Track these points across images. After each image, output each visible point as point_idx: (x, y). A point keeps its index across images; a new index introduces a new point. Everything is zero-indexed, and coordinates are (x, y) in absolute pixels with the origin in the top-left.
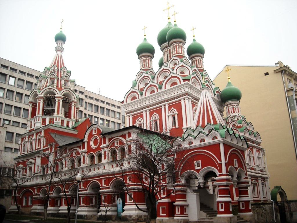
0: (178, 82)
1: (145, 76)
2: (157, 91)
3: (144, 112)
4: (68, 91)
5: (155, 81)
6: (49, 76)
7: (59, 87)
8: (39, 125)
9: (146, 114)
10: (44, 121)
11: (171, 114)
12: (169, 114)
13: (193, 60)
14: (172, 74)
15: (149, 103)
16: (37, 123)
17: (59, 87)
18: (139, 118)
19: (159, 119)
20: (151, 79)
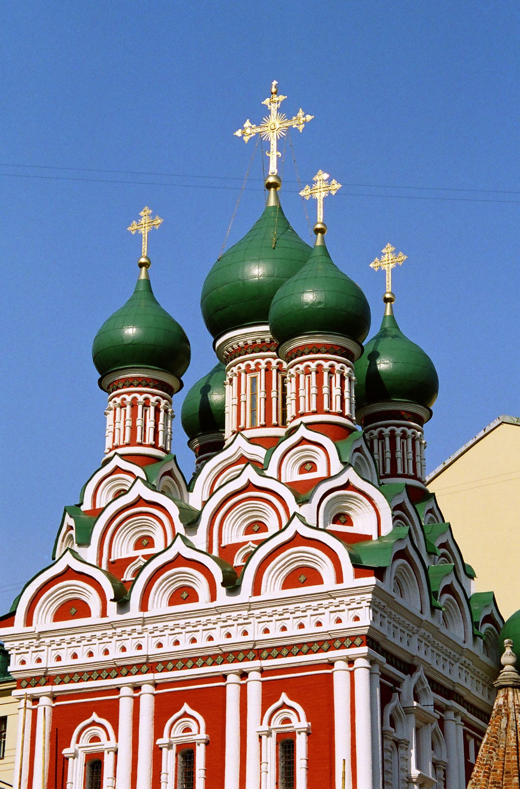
0: (327, 570)
1: (139, 501)
3: (126, 691)
5: (199, 539)
9: (137, 701)
11: (272, 726)
12: (265, 727)
13: (376, 433)
14: (296, 526)
15: (160, 650)
18: (95, 717)
19: (207, 744)
20: (180, 528)
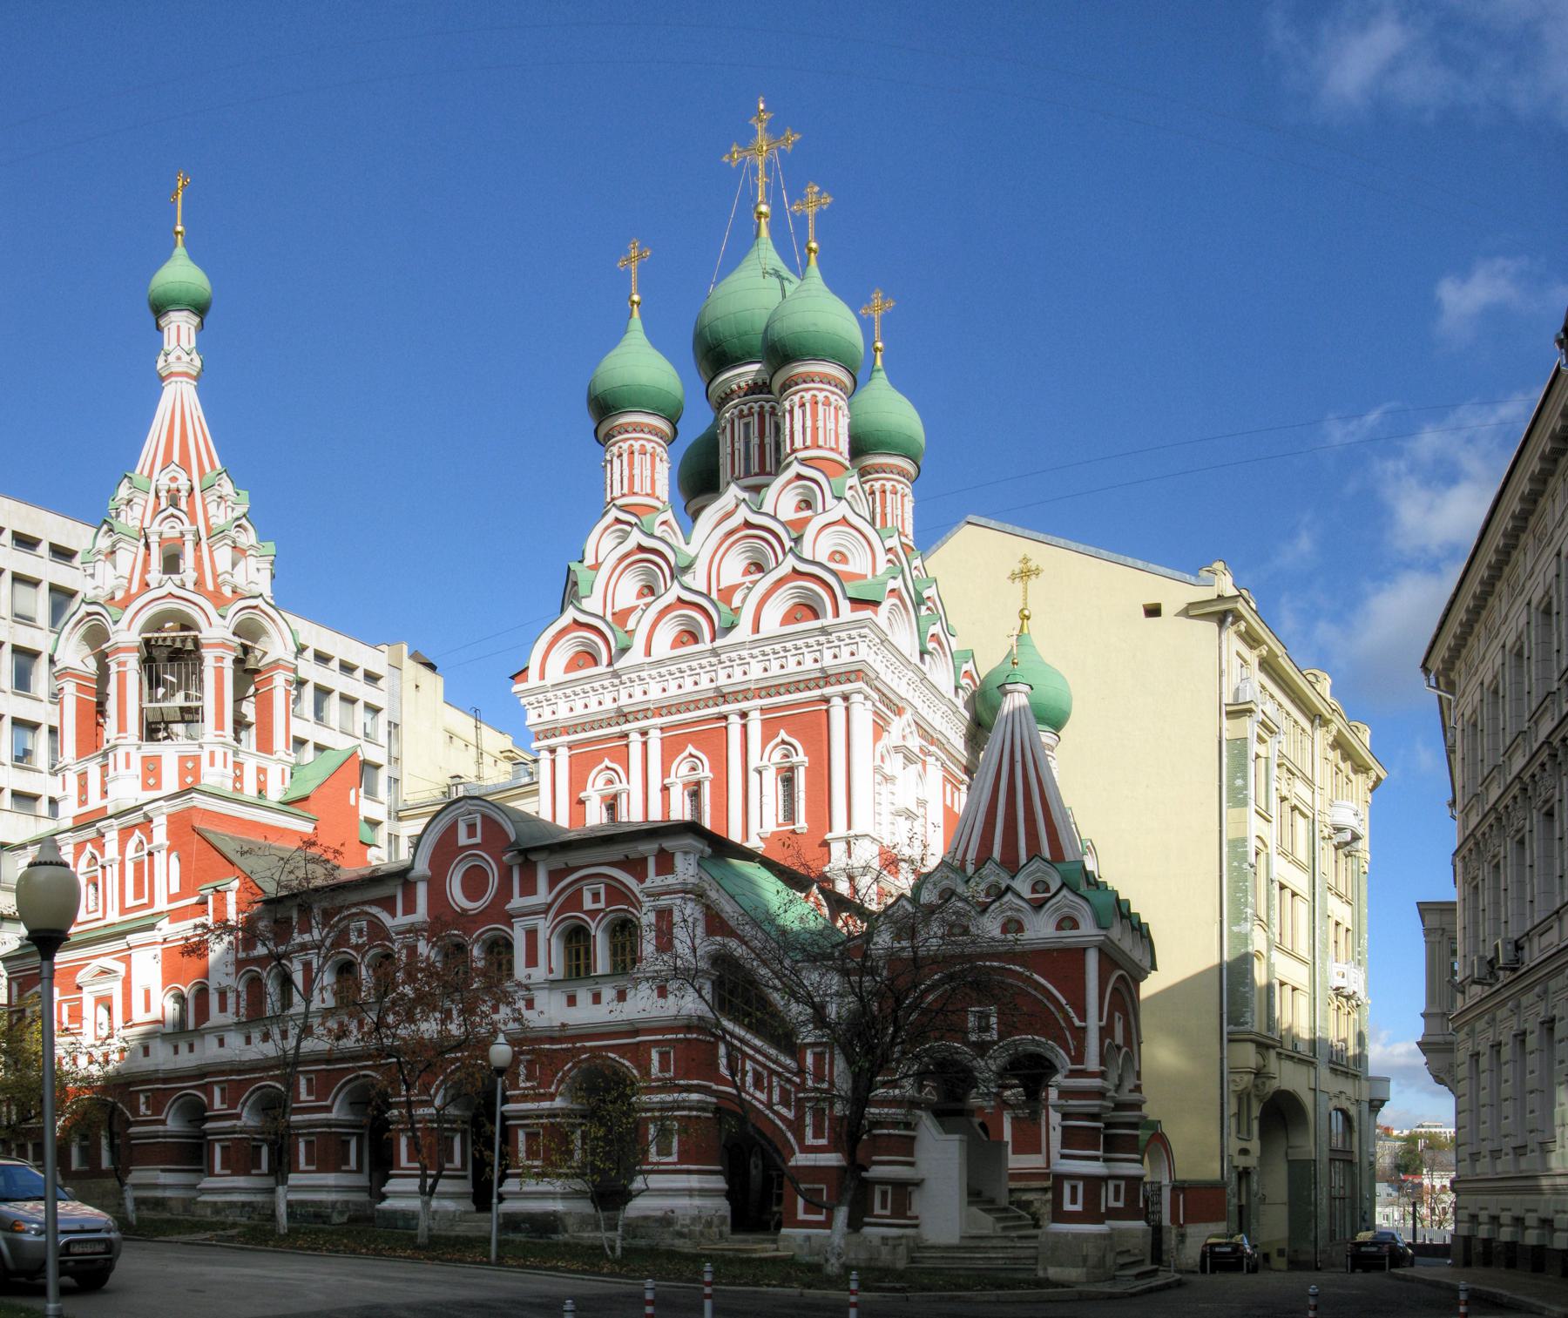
2: (713, 640)
4: (255, 607)
6: (155, 527)
7: (210, 587)
8: (127, 790)
10: (152, 769)
16: (116, 779)
17: (210, 587)
